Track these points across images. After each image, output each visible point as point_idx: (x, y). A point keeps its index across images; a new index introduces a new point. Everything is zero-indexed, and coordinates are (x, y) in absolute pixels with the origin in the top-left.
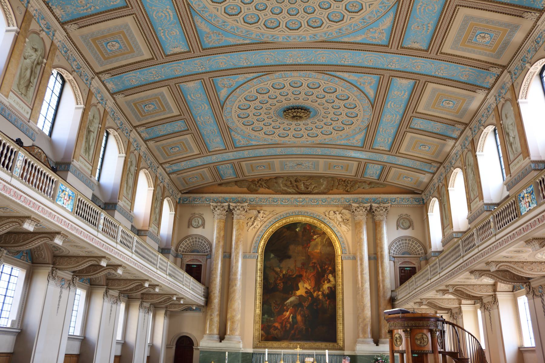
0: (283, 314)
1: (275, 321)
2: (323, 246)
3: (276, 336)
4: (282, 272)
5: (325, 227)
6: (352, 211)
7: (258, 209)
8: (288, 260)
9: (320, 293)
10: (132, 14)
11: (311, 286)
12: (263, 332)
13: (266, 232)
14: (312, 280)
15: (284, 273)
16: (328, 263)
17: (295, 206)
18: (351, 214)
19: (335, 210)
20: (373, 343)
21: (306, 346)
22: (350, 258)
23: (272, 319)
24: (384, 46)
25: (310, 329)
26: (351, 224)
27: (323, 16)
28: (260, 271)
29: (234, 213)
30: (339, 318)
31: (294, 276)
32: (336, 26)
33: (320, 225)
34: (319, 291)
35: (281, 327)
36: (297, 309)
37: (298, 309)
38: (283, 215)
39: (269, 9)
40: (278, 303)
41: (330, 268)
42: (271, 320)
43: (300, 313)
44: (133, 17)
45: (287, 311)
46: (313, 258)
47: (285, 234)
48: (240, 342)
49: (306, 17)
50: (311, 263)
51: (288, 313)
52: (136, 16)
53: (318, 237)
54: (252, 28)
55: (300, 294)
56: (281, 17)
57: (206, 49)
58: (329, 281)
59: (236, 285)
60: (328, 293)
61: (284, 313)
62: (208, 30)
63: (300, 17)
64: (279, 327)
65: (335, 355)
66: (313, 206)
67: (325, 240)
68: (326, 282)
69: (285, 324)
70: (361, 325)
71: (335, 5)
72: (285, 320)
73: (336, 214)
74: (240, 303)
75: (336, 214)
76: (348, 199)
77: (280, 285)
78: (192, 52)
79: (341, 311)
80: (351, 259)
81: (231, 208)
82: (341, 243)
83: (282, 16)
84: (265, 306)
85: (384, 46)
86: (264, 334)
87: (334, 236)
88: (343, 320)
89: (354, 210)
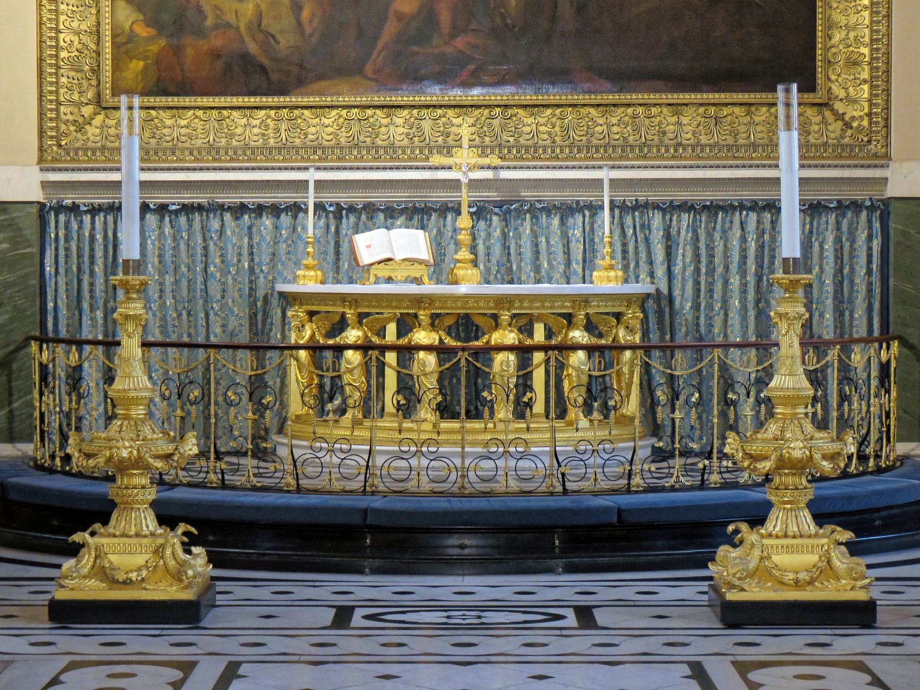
3: (252, 47)
86: (142, 31)
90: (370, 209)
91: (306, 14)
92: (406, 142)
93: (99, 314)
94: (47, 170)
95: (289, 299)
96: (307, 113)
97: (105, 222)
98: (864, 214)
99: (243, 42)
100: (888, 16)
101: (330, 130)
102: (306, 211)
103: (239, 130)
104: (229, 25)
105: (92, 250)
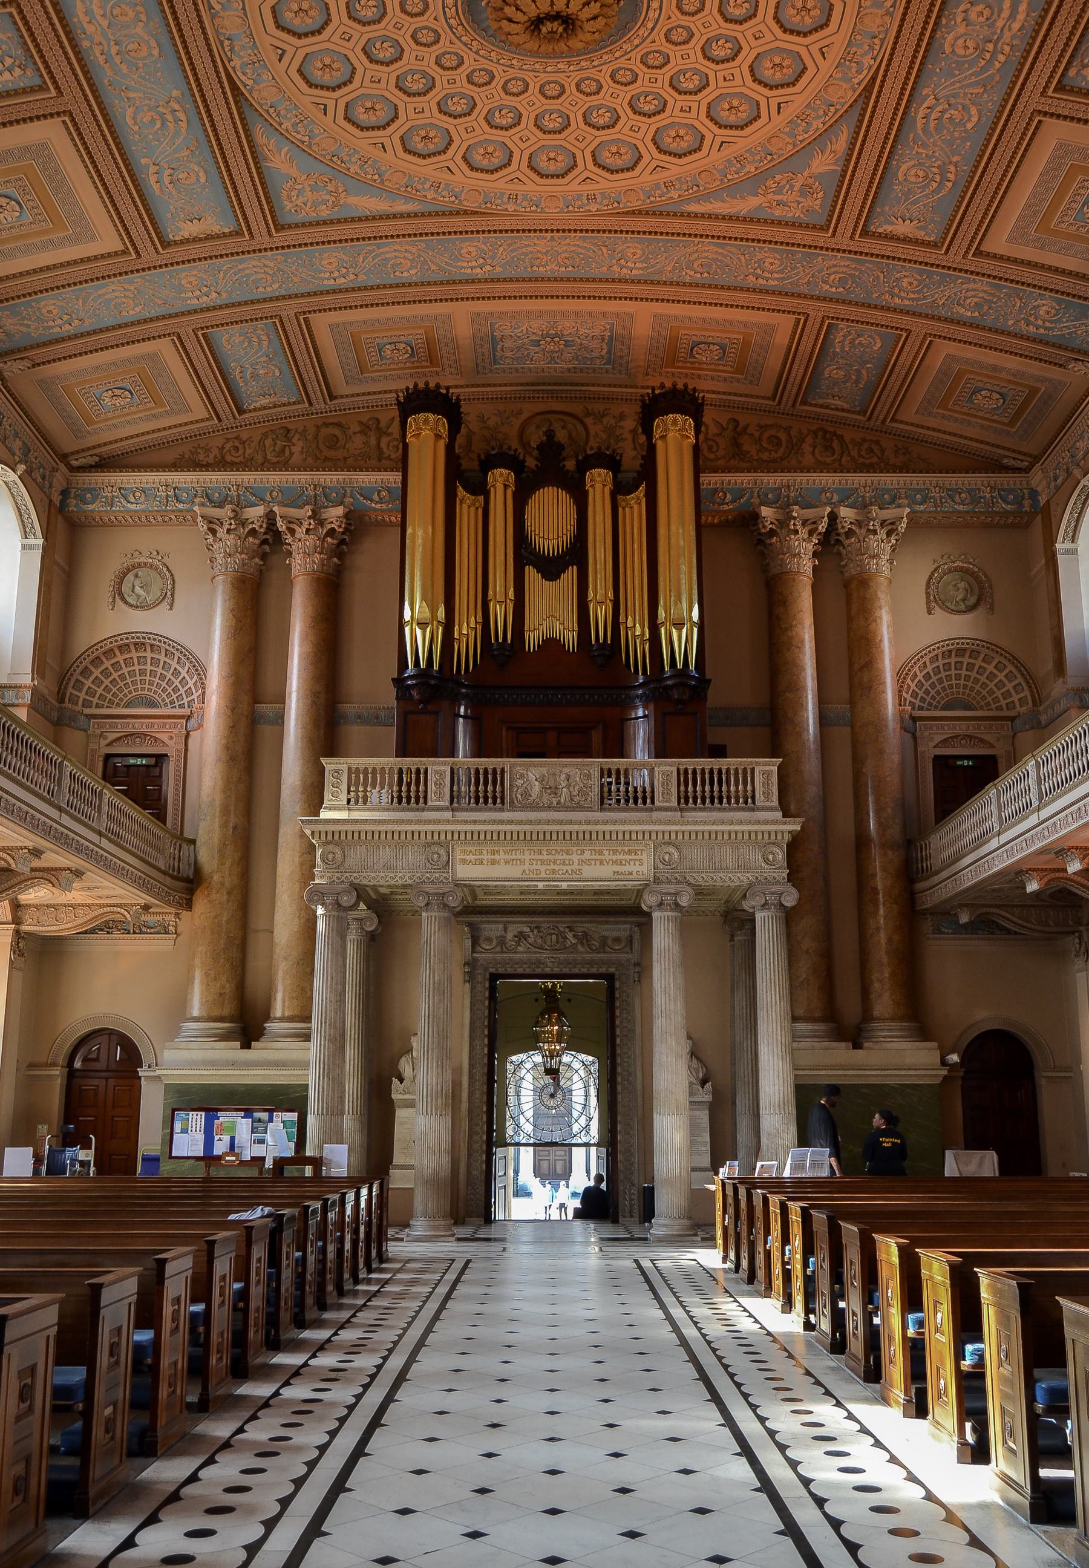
10: (58, 114)
24: (814, 227)
27: (640, 135)
32: (676, 168)
39: (481, 110)
44: (64, 122)
49: (589, 138)
52: (73, 120)
54: (427, 169)
56: (516, 138)
57: (290, 227)
62: (294, 172)
63: (571, 139)
71: (679, 105)
78: (247, 237)
83: (520, 135)
85: (814, 227)
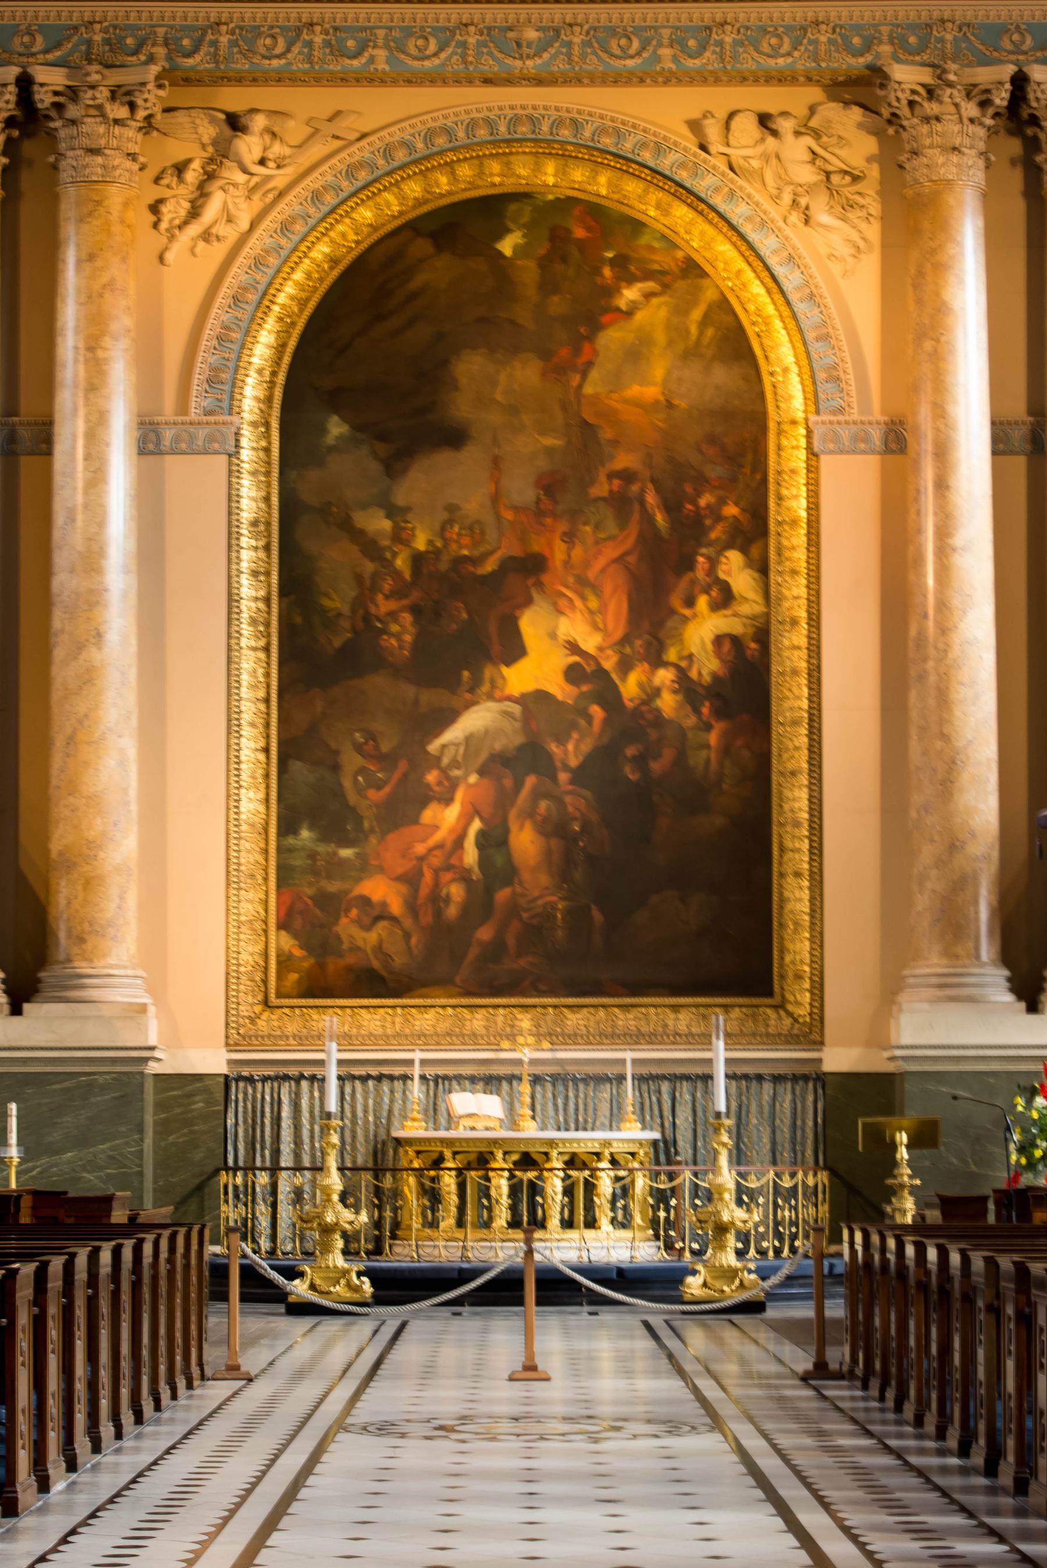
0: (415, 821)
1: (364, 868)
2: (689, 354)
3: (376, 964)
4: (406, 543)
5: (702, 225)
6: (886, 113)
7: (233, 99)
8: (444, 457)
9: (664, 676)
11: (606, 633)
12: (287, 942)
13: (288, 261)
14: (608, 589)
15: (420, 544)
16: (715, 472)
17: (488, 81)
18: (877, 133)
19: (771, 108)
20: (1009, 998)
21: (574, 1020)
22: (866, 439)
23: (346, 853)
25: (597, 916)
26: (875, 208)
28: (255, 536)
29: (62, 134)
30: (788, 844)
31: (489, 566)
33: (666, 213)
34: (657, 661)
35: (412, 907)
36: (508, 782)
37: (519, 785)
38: (404, 144)
40: (385, 747)
41: (731, 510)
42: (344, 862)
43: (530, 814)
45: (448, 801)
46: (615, 443)
47: (419, 280)
48: (143, 1009)
50: (602, 477)
51: (451, 814)
53: (648, 296)
55: (530, 687)
58: (725, 598)
59: (99, 635)
60: (715, 676)
61: (428, 815)
64: (396, 907)
65: (760, 1078)
66: (617, 79)
67: (697, 314)
68: (702, 602)
69: (437, 884)
70: (935, 883)
72: (436, 861)
73: (775, 133)
74: (132, 752)
75: (775, 133)
76: (858, 29)
77: (395, 628)
79: (803, 794)
80: (873, 452)
81: (43, 99)
82: (810, 336)
84: (296, 766)
86: (298, 952)
87: (757, 289)
88: (817, 851)
89: (905, 111)
90: (459, 1078)
91: (414, 941)
92: (483, 1031)
93: (267, 1153)
94: (231, 1051)
95: (398, 1142)
96: (413, 1010)
97: (272, 1089)
98: (811, 1085)
99: (368, 959)
100: (822, 946)
101: (430, 1023)
102: (412, 1079)
103: (365, 1023)
104: (358, 949)
105: (263, 1106)
